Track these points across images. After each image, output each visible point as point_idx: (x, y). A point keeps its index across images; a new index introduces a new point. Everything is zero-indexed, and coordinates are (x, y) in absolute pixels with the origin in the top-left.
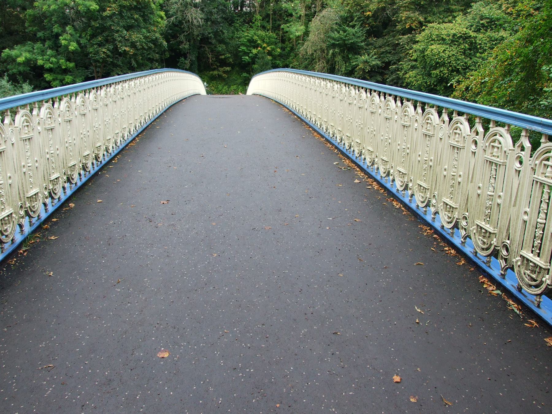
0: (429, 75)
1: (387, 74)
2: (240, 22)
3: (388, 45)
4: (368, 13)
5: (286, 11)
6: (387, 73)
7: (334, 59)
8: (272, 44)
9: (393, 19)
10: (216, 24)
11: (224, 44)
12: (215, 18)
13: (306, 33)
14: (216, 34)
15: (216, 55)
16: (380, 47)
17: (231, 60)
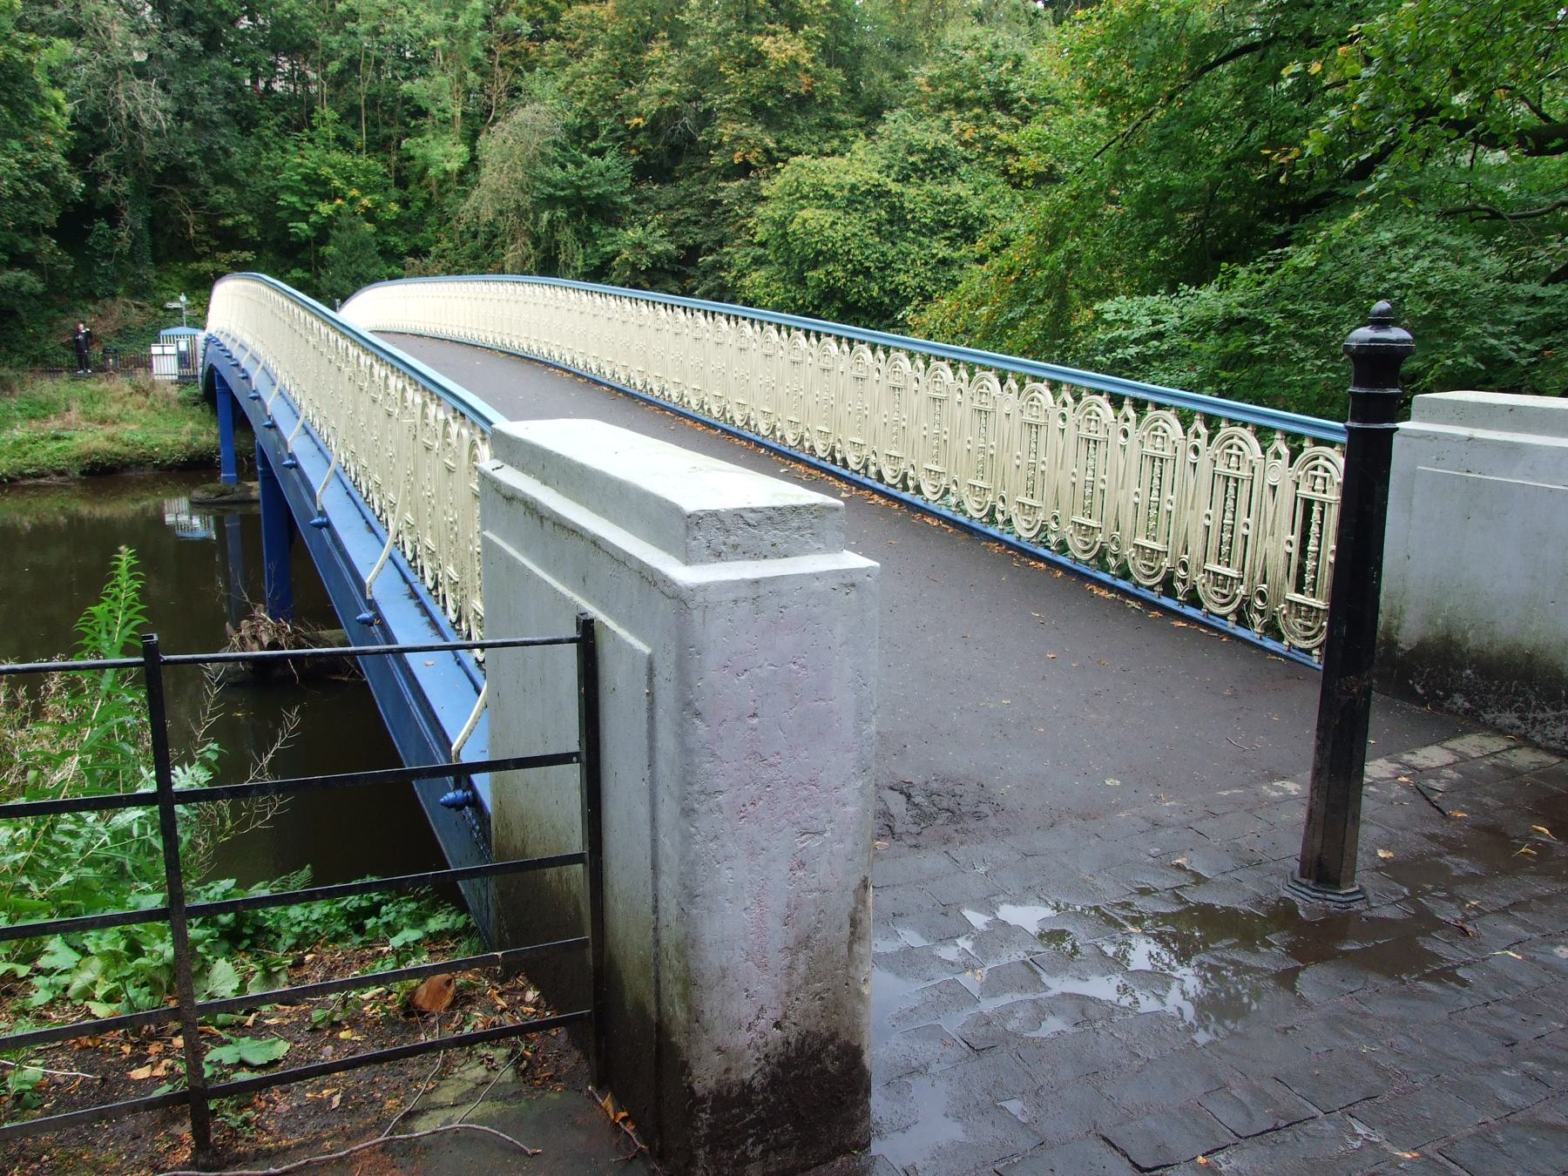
0: (801, 281)
1: (693, 277)
2: (277, 125)
3: (691, 202)
4: (636, 121)
5: (408, 100)
6: (693, 273)
7: (553, 236)
8: (373, 192)
9: (700, 139)
10: (206, 128)
11: (231, 185)
12: (206, 112)
13: (473, 163)
14: (208, 155)
15: (206, 216)
16: (670, 207)
17: (253, 232)
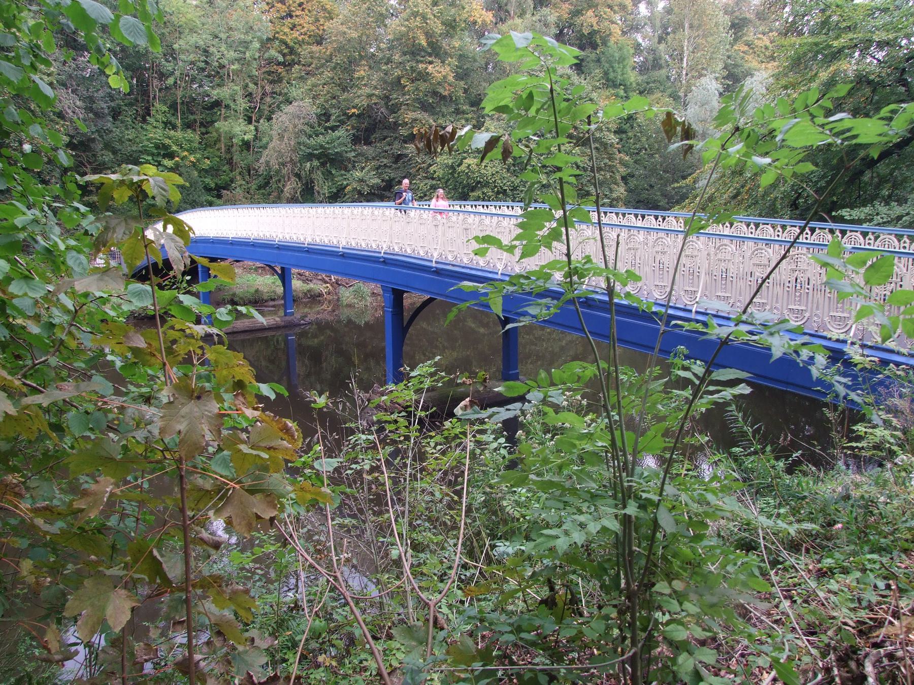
4: (353, 111)
